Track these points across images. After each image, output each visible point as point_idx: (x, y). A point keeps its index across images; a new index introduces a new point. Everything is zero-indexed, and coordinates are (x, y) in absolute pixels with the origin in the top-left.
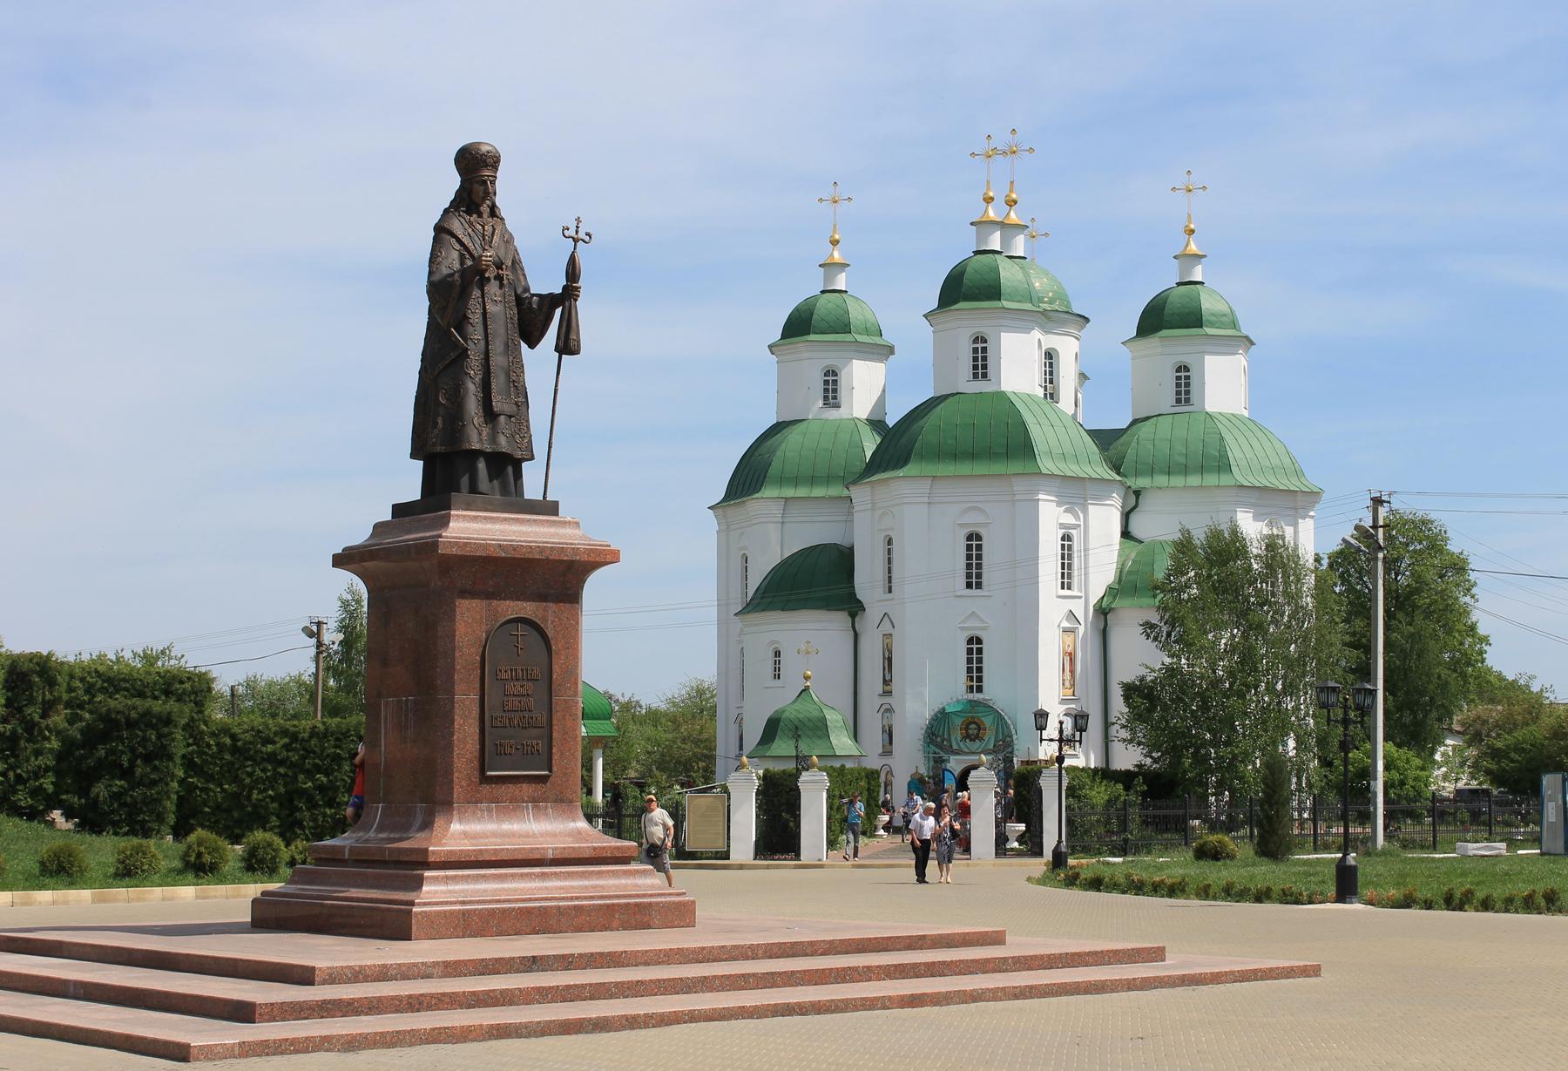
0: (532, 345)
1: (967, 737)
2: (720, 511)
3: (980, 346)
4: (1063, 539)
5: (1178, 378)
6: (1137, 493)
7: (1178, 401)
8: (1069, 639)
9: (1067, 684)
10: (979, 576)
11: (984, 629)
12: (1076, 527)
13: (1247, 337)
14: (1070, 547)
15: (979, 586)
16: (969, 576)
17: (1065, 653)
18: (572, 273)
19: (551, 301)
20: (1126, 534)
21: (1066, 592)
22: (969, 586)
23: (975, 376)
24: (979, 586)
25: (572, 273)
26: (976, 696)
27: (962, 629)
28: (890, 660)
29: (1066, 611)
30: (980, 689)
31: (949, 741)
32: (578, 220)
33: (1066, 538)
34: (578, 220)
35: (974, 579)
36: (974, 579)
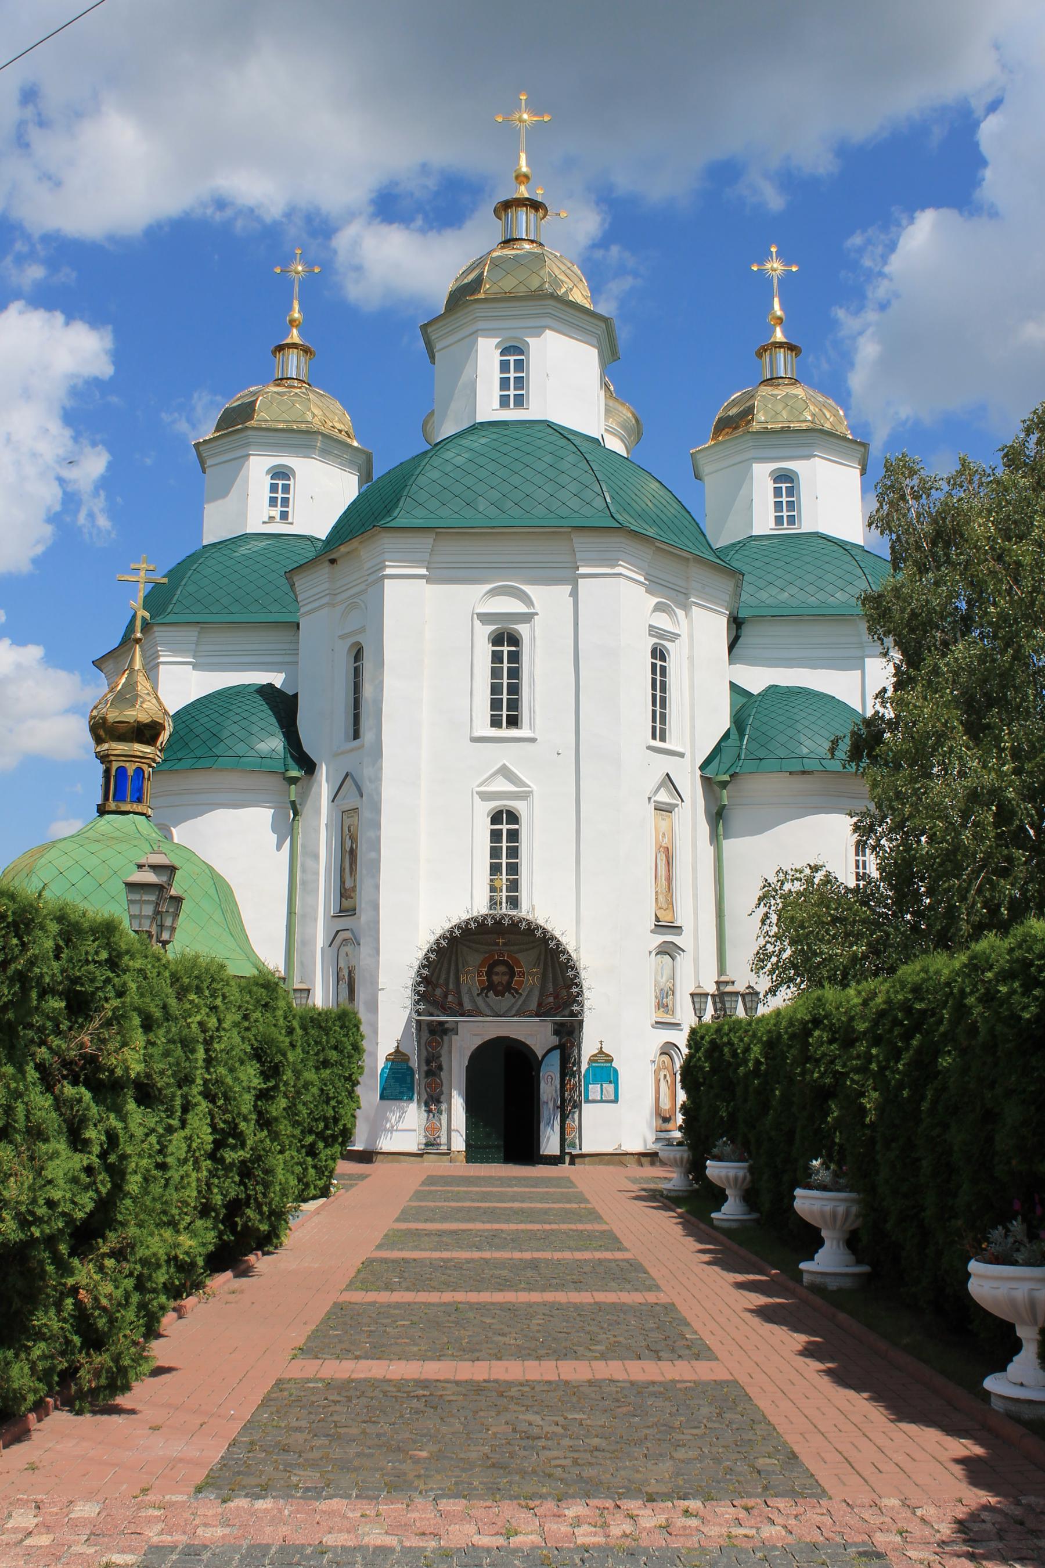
1: (490, 987)
2: (110, 665)
8: (664, 825)
9: (661, 898)
10: (514, 705)
11: (525, 796)
12: (673, 637)
14: (663, 669)
15: (513, 722)
16: (496, 705)
21: (657, 744)
22: (495, 722)
23: (504, 402)
24: (513, 722)
27: (485, 796)
28: (353, 853)
29: (660, 776)
30: (514, 902)
31: (458, 993)
33: (659, 654)
35: (507, 709)
36: (507, 709)
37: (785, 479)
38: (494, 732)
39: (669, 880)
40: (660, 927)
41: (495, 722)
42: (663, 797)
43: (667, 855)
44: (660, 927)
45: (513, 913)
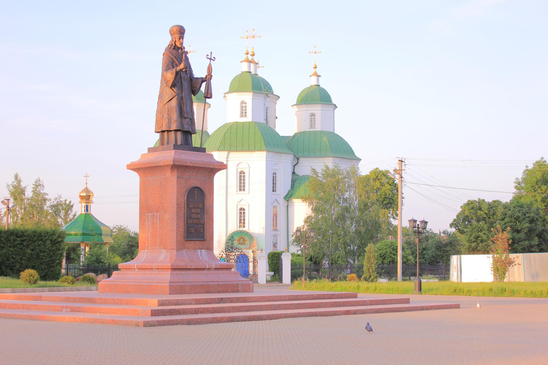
0: (194, 95)
3: (244, 105)
4: (273, 174)
5: (311, 119)
6: (298, 159)
7: (311, 126)
9: (275, 225)
10: (244, 186)
13: (335, 105)
16: (240, 186)
17: (274, 214)
18: (210, 69)
19: (203, 80)
20: (294, 173)
22: (240, 190)
24: (244, 190)
25: (210, 69)
26: (242, 229)
30: (244, 227)
32: (211, 53)
33: (275, 174)
34: (211, 53)
35: (242, 187)
36: (242, 187)
37: (313, 115)
38: (240, 192)
39: (276, 221)
40: (274, 230)
41: (240, 190)
42: (276, 204)
43: (275, 215)
44: (274, 230)
45: (244, 229)
